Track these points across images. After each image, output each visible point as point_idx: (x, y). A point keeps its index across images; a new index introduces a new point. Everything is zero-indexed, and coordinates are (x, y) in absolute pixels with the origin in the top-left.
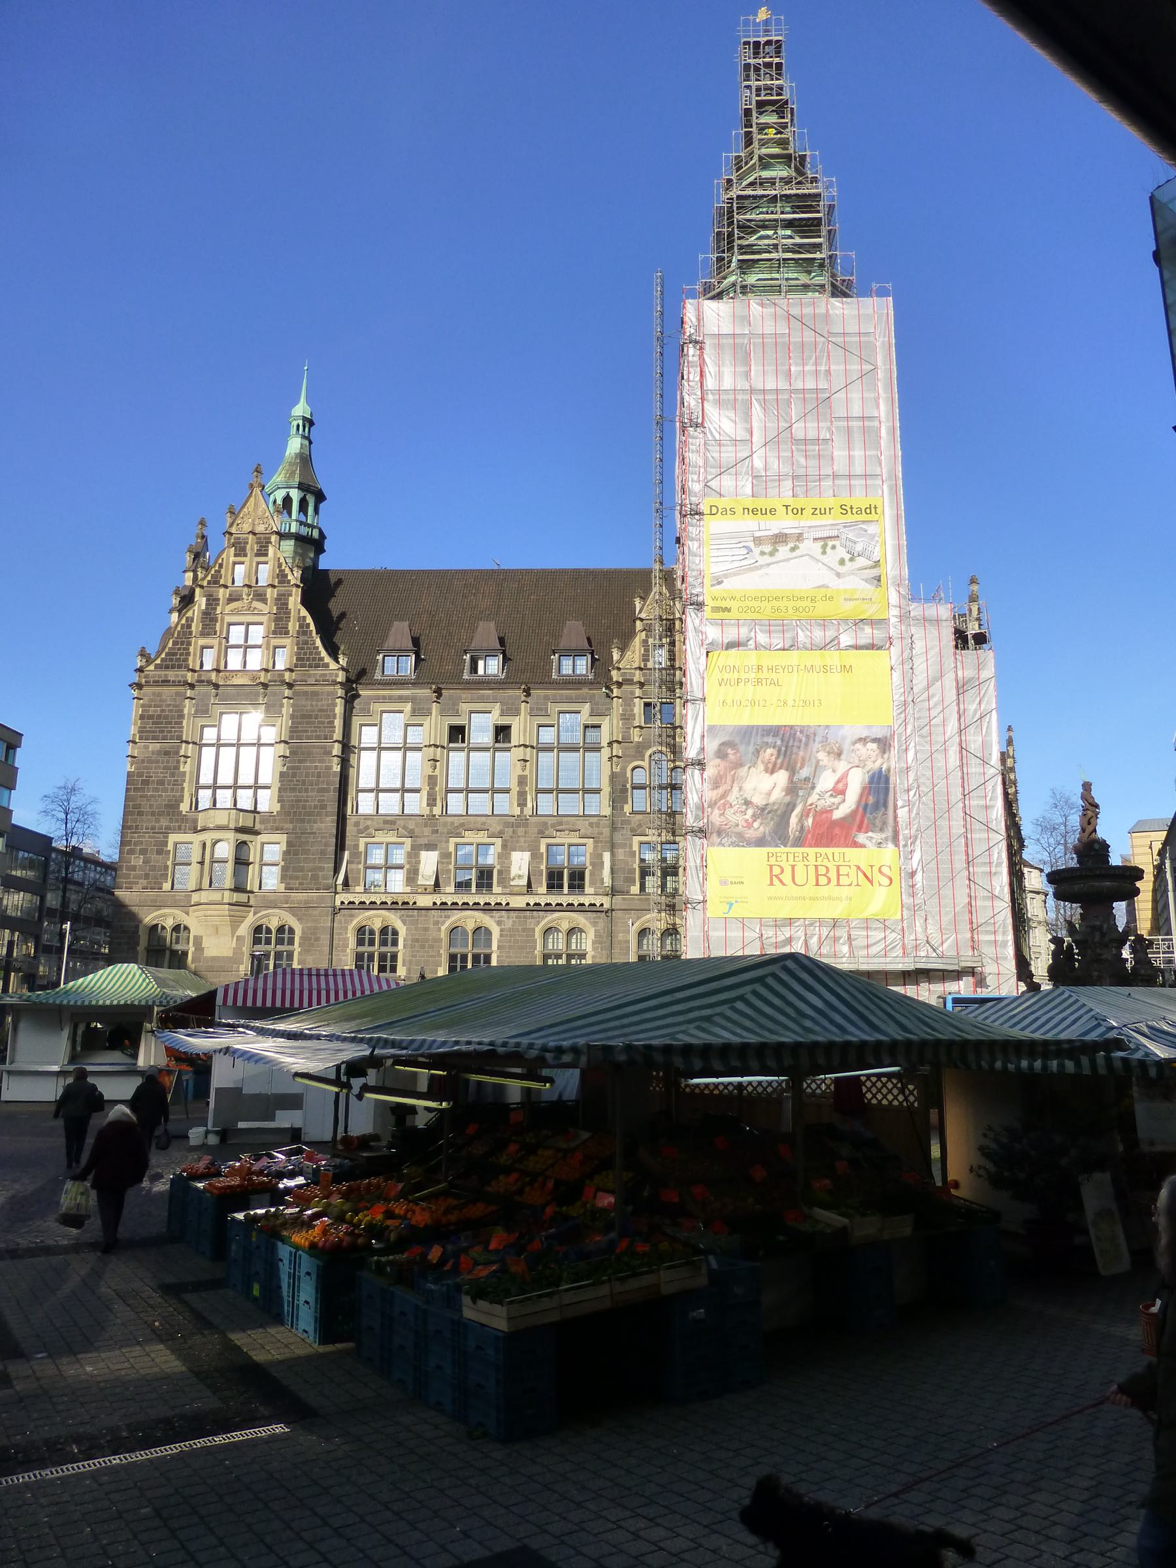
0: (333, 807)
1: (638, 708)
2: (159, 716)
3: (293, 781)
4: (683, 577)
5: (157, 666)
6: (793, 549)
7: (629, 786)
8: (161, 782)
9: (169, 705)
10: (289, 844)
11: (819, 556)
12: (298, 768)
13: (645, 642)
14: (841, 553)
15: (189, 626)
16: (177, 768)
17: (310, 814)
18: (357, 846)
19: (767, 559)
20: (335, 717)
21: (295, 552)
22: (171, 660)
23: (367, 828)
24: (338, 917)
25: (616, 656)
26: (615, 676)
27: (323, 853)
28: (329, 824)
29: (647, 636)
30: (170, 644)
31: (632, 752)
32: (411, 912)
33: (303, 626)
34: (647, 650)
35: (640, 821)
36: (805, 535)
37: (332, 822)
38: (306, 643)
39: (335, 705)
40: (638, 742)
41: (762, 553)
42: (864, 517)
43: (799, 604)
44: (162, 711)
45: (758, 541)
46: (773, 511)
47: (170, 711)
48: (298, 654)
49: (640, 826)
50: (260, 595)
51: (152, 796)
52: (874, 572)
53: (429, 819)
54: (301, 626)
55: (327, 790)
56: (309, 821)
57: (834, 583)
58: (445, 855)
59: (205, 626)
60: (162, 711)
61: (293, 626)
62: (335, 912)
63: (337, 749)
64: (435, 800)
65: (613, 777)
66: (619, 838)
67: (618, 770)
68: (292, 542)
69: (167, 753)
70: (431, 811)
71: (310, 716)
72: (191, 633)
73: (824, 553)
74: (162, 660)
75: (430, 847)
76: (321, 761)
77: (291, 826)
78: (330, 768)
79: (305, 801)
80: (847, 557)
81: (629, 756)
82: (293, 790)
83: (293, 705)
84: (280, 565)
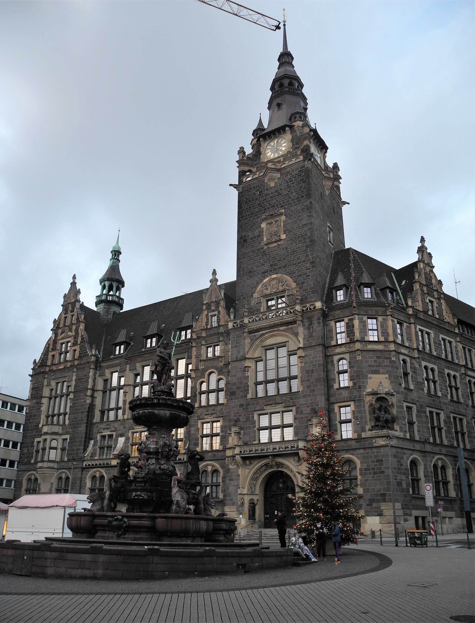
0: (85, 421)
3: (73, 409)
7: (197, 393)
8: (35, 416)
10: (70, 439)
12: (75, 403)
13: (207, 315)
15: (49, 347)
16: (40, 409)
17: (78, 424)
18: (97, 437)
21: (104, 308)
23: (100, 428)
24: (84, 472)
27: (81, 442)
28: (82, 428)
29: (208, 312)
31: (199, 374)
32: (108, 469)
33: (83, 339)
34: (208, 320)
35: (202, 411)
37: (84, 427)
39: (89, 372)
40: (203, 369)
49: (201, 414)
50: (71, 329)
51: (32, 422)
53: (123, 422)
55: (83, 412)
56: (77, 427)
58: (127, 439)
61: (79, 340)
62: (83, 469)
63: (89, 393)
64: (125, 412)
67: (193, 385)
68: (103, 304)
69: (38, 403)
70: (123, 417)
71: (81, 379)
75: (122, 436)
76: (83, 399)
77: (71, 430)
78: (85, 401)
79: (77, 418)
81: (198, 377)
82: (73, 413)
83: (76, 375)
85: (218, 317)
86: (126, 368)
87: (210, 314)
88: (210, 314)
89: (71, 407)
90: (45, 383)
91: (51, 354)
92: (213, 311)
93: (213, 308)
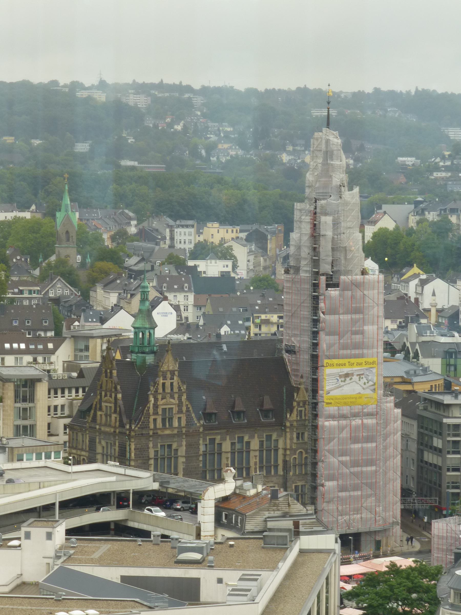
1: (295, 436)
2: (141, 449)
4: (331, 403)
5: (139, 428)
6: (351, 379)
9: (144, 444)
11: (358, 382)
13: (297, 409)
14: (365, 380)
15: (149, 410)
19: (343, 383)
20: (199, 444)
22: (143, 425)
25: (288, 416)
26: (288, 424)
30: (143, 419)
33: (188, 408)
34: (297, 413)
36: (354, 374)
38: (189, 415)
41: (342, 381)
42: (372, 366)
43: (352, 400)
44: (142, 446)
45: (340, 376)
46: (345, 365)
47: (144, 446)
48: (186, 420)
52: (373, 387)
54: (187, 408)
57: (362, 392)
59: (154, 410)
60: (142, 446)
61: (184, 409)
65: (285, 462)
66: (288, 484)
72: (149, 413)
73: (360, 380)
74: (141, 425)
78: (199, 465)
80: (366, 381)
83: (186, 441)
84: (178, 383)
85: (305, 412)
86: (226, 437)
87: (299, 409)
88: (299, 409)
89: (184, 469)
90: (151, 445)
91: (152, 418)
92: (301, 407)
93: (301, 405)
